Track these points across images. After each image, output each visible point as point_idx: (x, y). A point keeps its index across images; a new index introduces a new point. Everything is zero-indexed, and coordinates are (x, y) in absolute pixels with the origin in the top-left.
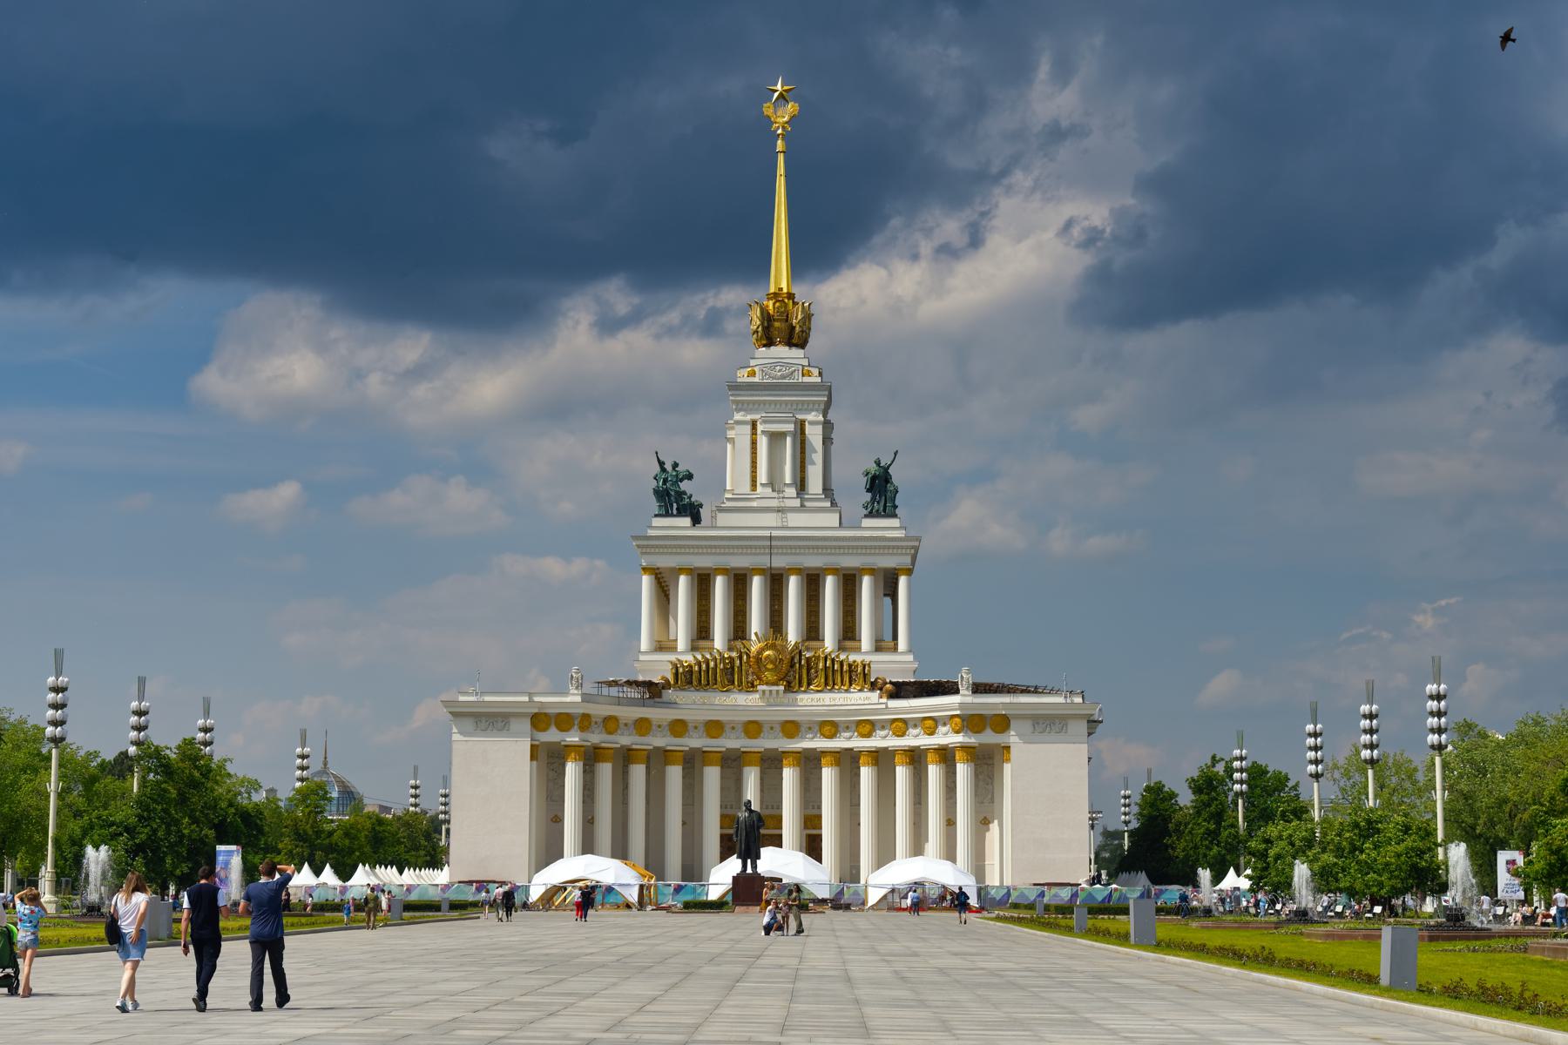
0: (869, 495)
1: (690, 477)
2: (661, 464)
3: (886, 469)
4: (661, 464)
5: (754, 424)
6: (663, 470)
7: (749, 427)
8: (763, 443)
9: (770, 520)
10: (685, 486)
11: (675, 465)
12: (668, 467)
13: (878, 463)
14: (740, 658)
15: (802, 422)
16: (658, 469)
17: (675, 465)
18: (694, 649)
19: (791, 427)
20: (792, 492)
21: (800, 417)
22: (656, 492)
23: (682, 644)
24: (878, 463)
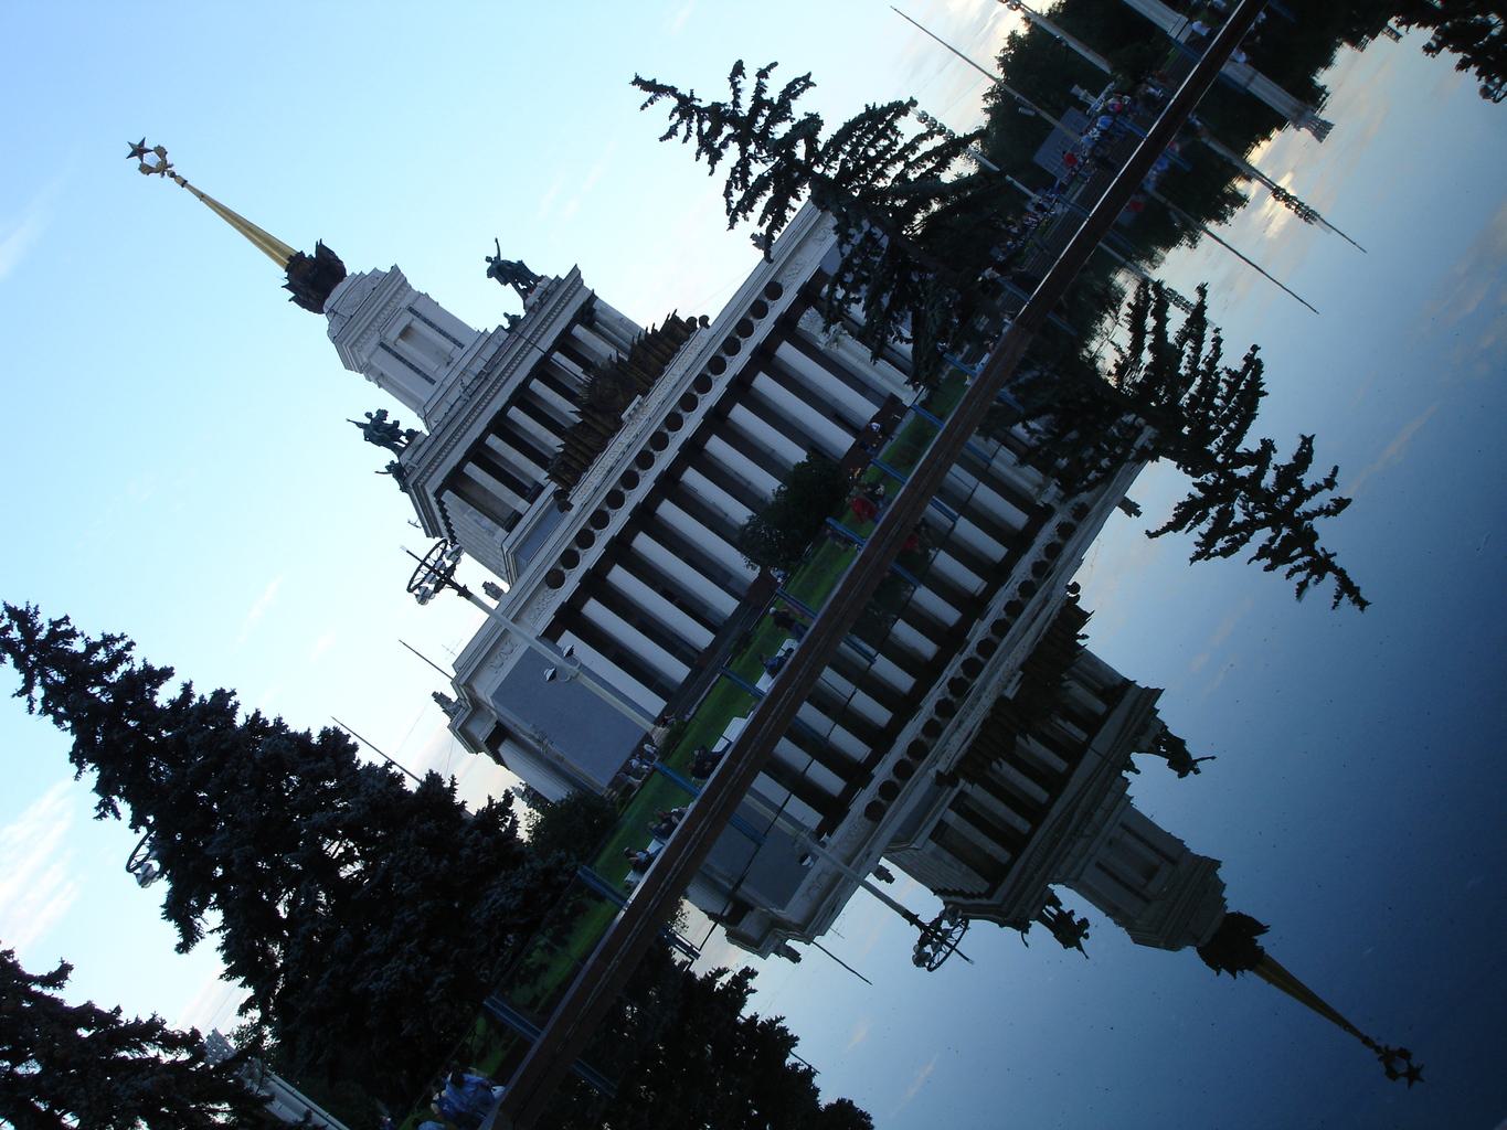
0: (509, 284)
2: (360, 425)
4: (360, 425)
8: (405, 347)
10: (389, 421)
11: (368, 415)
12: (368, 421)
13: (488, 259)
15: (411, 310)
16: (362, 431)
17: (368, 415)
18: (532, 502)
19: (407, 318)
20: (458, 353)
21: (404, 305)
23: (521, 504)
24: (488, 259)
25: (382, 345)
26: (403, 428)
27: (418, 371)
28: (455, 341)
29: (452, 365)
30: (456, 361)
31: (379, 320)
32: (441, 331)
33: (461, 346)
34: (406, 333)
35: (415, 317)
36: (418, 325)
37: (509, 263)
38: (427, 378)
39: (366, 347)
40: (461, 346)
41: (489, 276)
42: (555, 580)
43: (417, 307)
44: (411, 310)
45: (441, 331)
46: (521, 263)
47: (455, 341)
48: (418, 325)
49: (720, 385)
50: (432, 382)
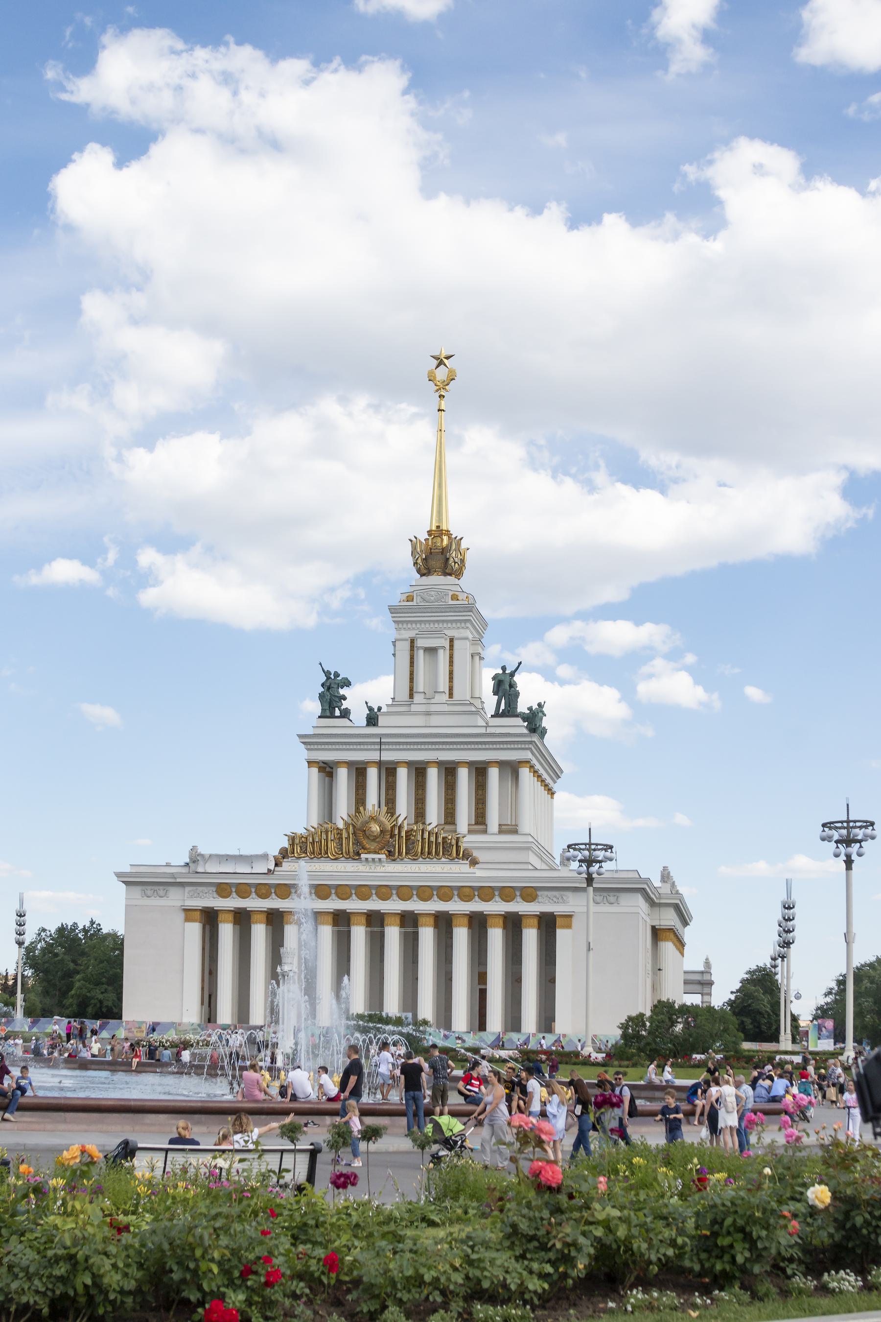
0: (496, 697)
1: (347, 683)
2: (327, 674)
3: (512, 674)
5: (412, 641)
6: (328, 678)
7: (407, 645)
9: (419, 720)
14: (347, 829)
15: (452, 641)
17: (337, 675)
21: (450, 633)
22: (321, 696)
24: (504, 668)
25: (412, 641)
26: (345, 704)
27: (412, 680)
28: (451, 689)
29: (429, 701)
30: (433, 701)
31: (423, 626)
32: (451, 673)
33: (451, 695)
34: (431, 651)
35: (448, 647)
36: (443, 657)
37: (512, 685)
38: (411, 689)
39: (403, 632)
40: (451, 695)
41: (494, 678)
42: (223, 890)
43: (456, 643)
44: (452, 641)
45: (451, 673)
46: (517, 694)
47: (451, 689)
48: (443, 657)
49: (435, 906)
50: (411, 696)
